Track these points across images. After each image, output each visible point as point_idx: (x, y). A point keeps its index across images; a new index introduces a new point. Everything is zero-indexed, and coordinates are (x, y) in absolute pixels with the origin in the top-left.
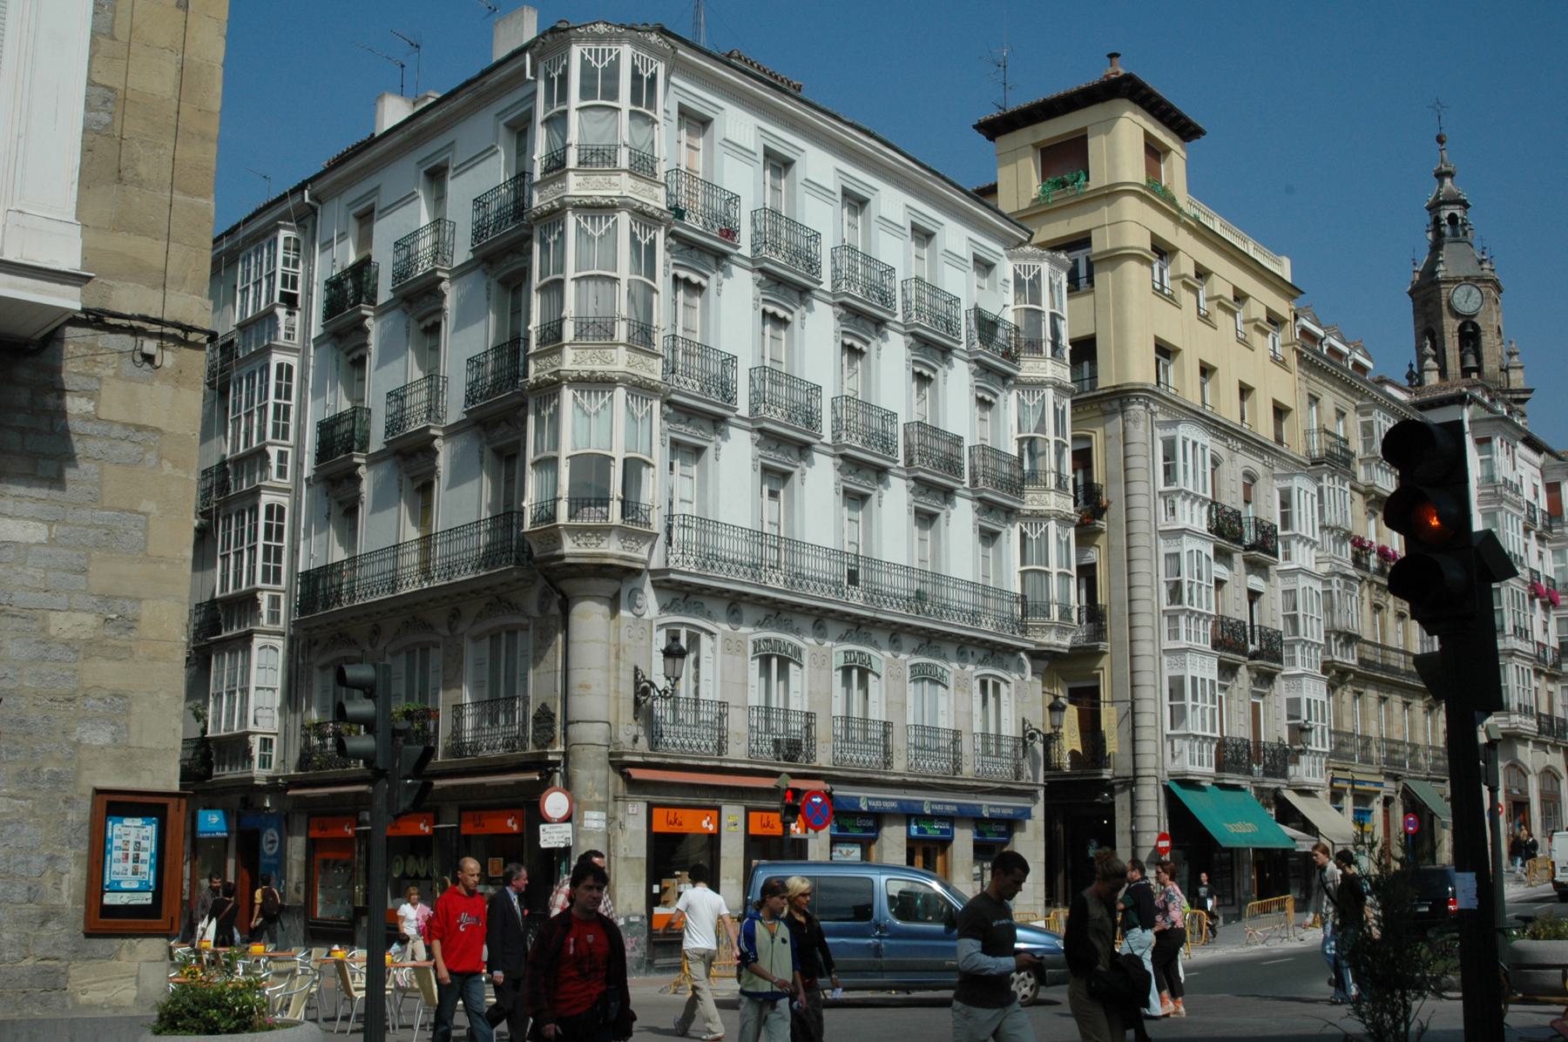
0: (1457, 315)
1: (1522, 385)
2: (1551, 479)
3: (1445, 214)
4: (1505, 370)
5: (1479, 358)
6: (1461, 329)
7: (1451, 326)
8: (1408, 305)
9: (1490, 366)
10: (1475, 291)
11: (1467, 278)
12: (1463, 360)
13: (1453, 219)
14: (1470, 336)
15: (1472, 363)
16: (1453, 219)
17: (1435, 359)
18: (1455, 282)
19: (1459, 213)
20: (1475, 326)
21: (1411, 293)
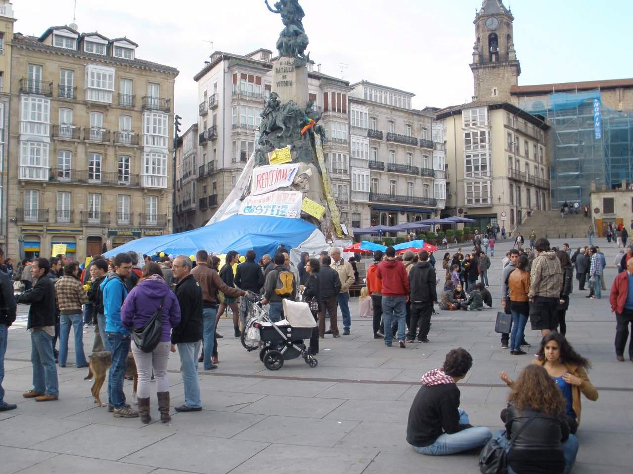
2: (325, 91)
4: (508, 54)
6: (490, 35)
8: (473, 26)
9: (501, 50)
10: (495, 20)
20: (496, 36)
21: (475, 22)
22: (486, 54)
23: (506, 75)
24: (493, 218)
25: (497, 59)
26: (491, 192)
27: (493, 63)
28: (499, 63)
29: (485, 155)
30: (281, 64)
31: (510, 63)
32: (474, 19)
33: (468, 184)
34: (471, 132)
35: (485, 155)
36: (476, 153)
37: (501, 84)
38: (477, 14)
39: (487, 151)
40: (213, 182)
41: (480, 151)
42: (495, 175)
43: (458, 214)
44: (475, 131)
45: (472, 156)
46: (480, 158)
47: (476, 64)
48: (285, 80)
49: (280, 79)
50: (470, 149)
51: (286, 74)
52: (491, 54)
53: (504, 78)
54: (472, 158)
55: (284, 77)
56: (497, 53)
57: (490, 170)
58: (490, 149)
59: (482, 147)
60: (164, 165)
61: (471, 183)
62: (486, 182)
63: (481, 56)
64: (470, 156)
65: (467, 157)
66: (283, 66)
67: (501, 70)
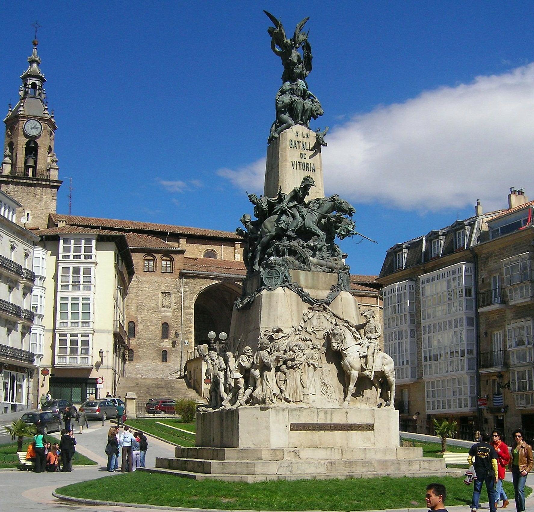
0: (26, 136)
1: (56, 178)
3: (30, 82)
5: (36, 162)
6: (28, 144)
7: (22, 141)
9: (41, 166)
11: (34, 117)
12: (26, 162)
13: (34, 85)
14: (32, 149)
15: (31, 163)
16: (34, 85)
17: (11, 157)
18: (28, 118)
19: (38, 83)
20: (36, 144)
22: (21, 164)
23: (44, 197)
27: (30, 179)
28: (38, 180)
31: (52, 184)
33: (60, 335)
36: (76, 295)
37: (36, 207)
41: (81, 294)
43: (41, 377)
44: (76, 265)
47: (7, 177)
48: (303, 161)
49: (297, 159)
52: (27, 168)
54: (70, 302)
56: (35, 168)
61: (66, 335)
62: (88, 336)
63: (14, 166)
66: (300, 138)
67: (39, 190)
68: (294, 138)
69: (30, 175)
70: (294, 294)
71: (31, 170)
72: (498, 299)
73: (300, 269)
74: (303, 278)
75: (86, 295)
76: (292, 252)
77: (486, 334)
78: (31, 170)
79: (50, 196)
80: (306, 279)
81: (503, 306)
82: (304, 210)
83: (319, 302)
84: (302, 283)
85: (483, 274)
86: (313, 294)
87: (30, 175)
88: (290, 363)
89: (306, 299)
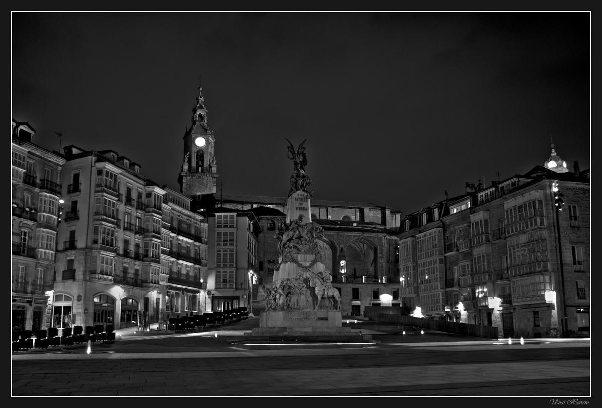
21: (184, 138)
22: (194, 164)
23: (209, 184)
24: (235, 299)
25: (202, 171)
26: (236, 279)
29: (233, 251)
30: (298, 195)
32: (183, 136)
34: (222, 232)
35: (233, 251)
36: (225, 248)
38: (186, 131)
39: (234, 248)
40: (69, 258)
42: (239, 266)
45: (222, 251)
46: (228, 253)
48: (301, 206)
49: (298, 205)
50: (227, 245)
51: (302, 202)
53: (206, 187)
54: (222, 253)
55: (301, 204)
56: (202, 166)
57: (236, 262)
58: (236, 247)
59: (232, 245)
60: (53, 243)
64: (220, 251)
65: (218, 251)
68: (297, 197)
69: (200, 170)
70: (295, 265)
71: (200, 169)
72: (455, 249)
73: (298, 253)
74: (300, 257)
75: (231, 248)
76: (295, 247)
77: (450, 268)
78: (200, 169)
79: (212, 183)
80: (301, 257)
81: (457, 253)
82: (300, 229)
83: (306, 268)
84: (299, 259)
85: (448, 234)
86: (304, 264)
87: (200, 170)
88: (292, 293)
89: (299, 265)
